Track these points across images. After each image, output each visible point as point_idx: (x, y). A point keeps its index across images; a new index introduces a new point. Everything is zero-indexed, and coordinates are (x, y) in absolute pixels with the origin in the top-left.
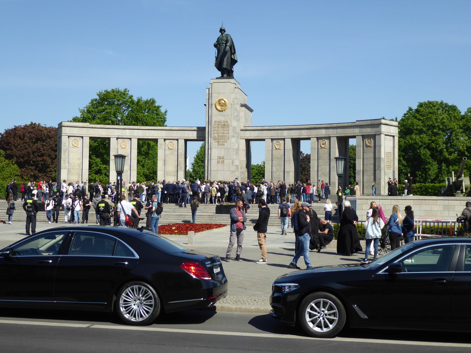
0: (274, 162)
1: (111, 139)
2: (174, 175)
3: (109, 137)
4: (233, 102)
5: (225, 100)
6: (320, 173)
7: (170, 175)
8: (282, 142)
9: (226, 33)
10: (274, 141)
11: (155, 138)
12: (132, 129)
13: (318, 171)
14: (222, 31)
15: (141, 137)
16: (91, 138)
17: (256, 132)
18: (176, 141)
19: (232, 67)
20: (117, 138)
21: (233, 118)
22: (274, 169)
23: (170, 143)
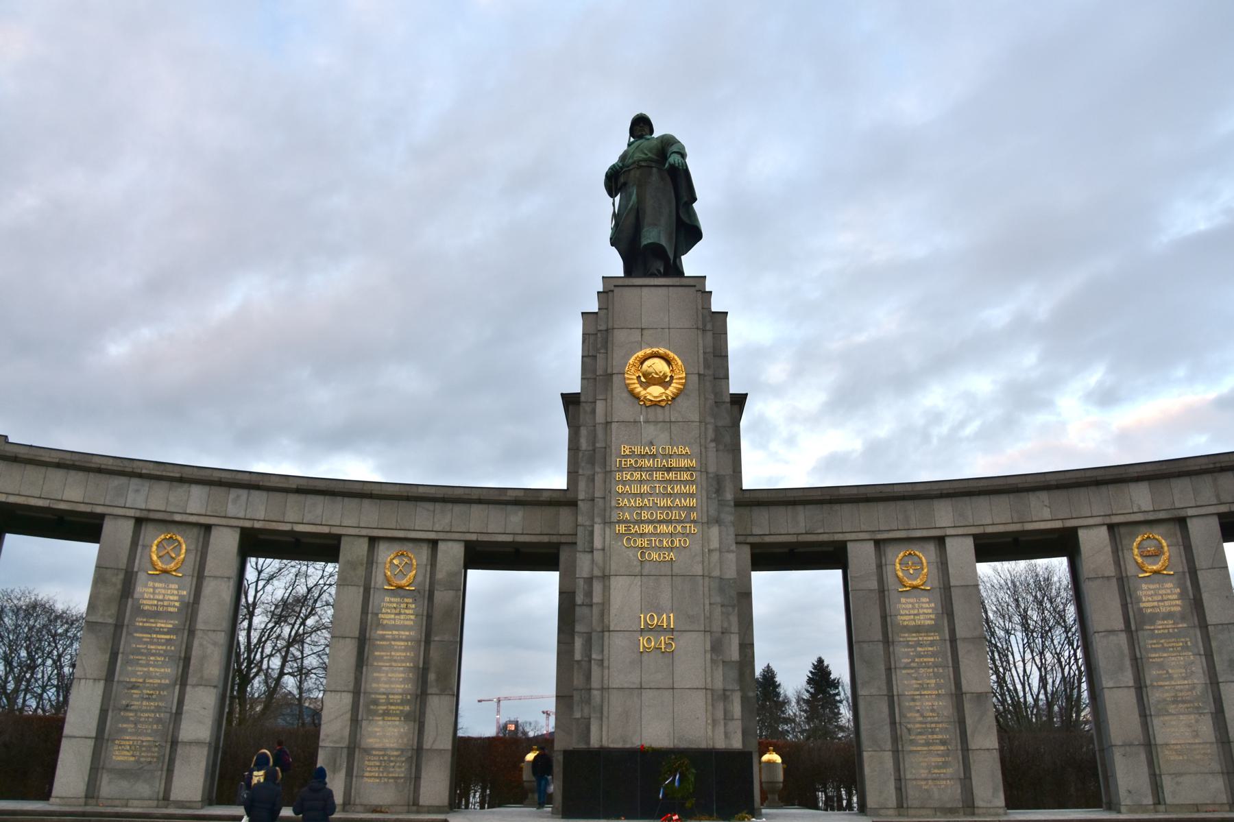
0: (900, 650)
1: (108, 527)
2: (407, 717)
3: (99, 510)
4: (707, 365)
5: (672, 355)
6: (1154, 696)
7: (386, 714)
8: (926, 556)
9: (655, 135)
10: (890, 551)
11: (326, 530)
13: (1140, 688)
14: (641, 125)
15: (257, 525)
17: (800, 508)
18: (425, 551)
20: (139, 522)
21: (711, 434)
22: (905, 683)
23: (396, 562)
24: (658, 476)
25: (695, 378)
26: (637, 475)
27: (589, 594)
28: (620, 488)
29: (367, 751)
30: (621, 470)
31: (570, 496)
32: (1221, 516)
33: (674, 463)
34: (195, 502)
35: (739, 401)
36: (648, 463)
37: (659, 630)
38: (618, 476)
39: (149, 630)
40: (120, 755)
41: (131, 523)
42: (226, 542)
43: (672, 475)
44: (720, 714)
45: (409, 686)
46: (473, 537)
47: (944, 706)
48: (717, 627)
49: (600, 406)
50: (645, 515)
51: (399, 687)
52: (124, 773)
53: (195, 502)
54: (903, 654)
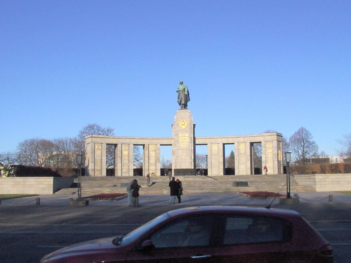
1: (118, 144)
3: (117, 143)
6: (240, 163)
12: (130, 139)
16: (107, 144)
19: (187, 104)
21: (190, 132)
24: (184, 137)
25: (188, 125)
26: (182, 137)
27: (176, 152)
28: (180, 139)
29: (150, 169)
30: (180, 137)
31: (173, 138)
32: (250, 142)
33: (186, 136)
34: (128, 141)
35: (194, 125)
36: (183, 136)
37: (184, 156)
38: (179, 137)
39: (125, 157)
40: (124, 171)
41: (121, 145)
42: (132, 146)
43: (186, 137)
44: (191, 165)
45: (155, 162)
46: (161, 144)
47: (218, 163)
48: (191, 155)
49: (177, 128)
50: (183, 142)
51: (154, 162)
52: (125, 173)
53: (128, 141)
54: (213, 157)
